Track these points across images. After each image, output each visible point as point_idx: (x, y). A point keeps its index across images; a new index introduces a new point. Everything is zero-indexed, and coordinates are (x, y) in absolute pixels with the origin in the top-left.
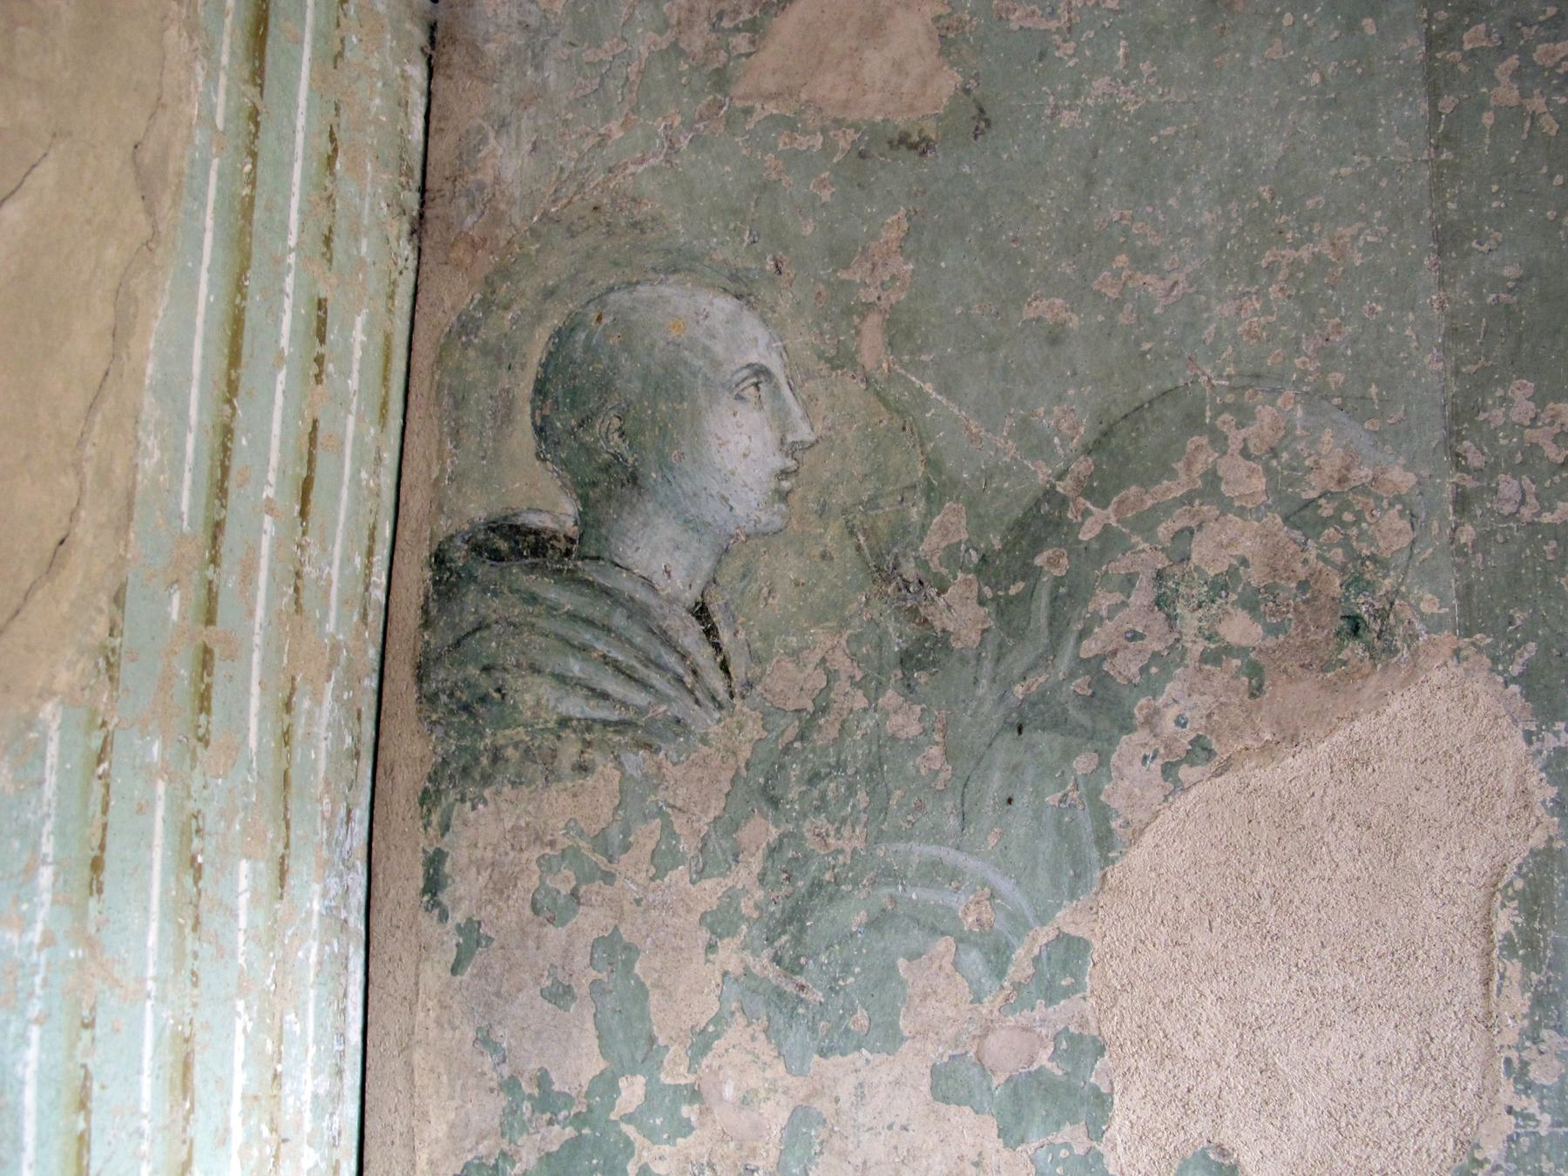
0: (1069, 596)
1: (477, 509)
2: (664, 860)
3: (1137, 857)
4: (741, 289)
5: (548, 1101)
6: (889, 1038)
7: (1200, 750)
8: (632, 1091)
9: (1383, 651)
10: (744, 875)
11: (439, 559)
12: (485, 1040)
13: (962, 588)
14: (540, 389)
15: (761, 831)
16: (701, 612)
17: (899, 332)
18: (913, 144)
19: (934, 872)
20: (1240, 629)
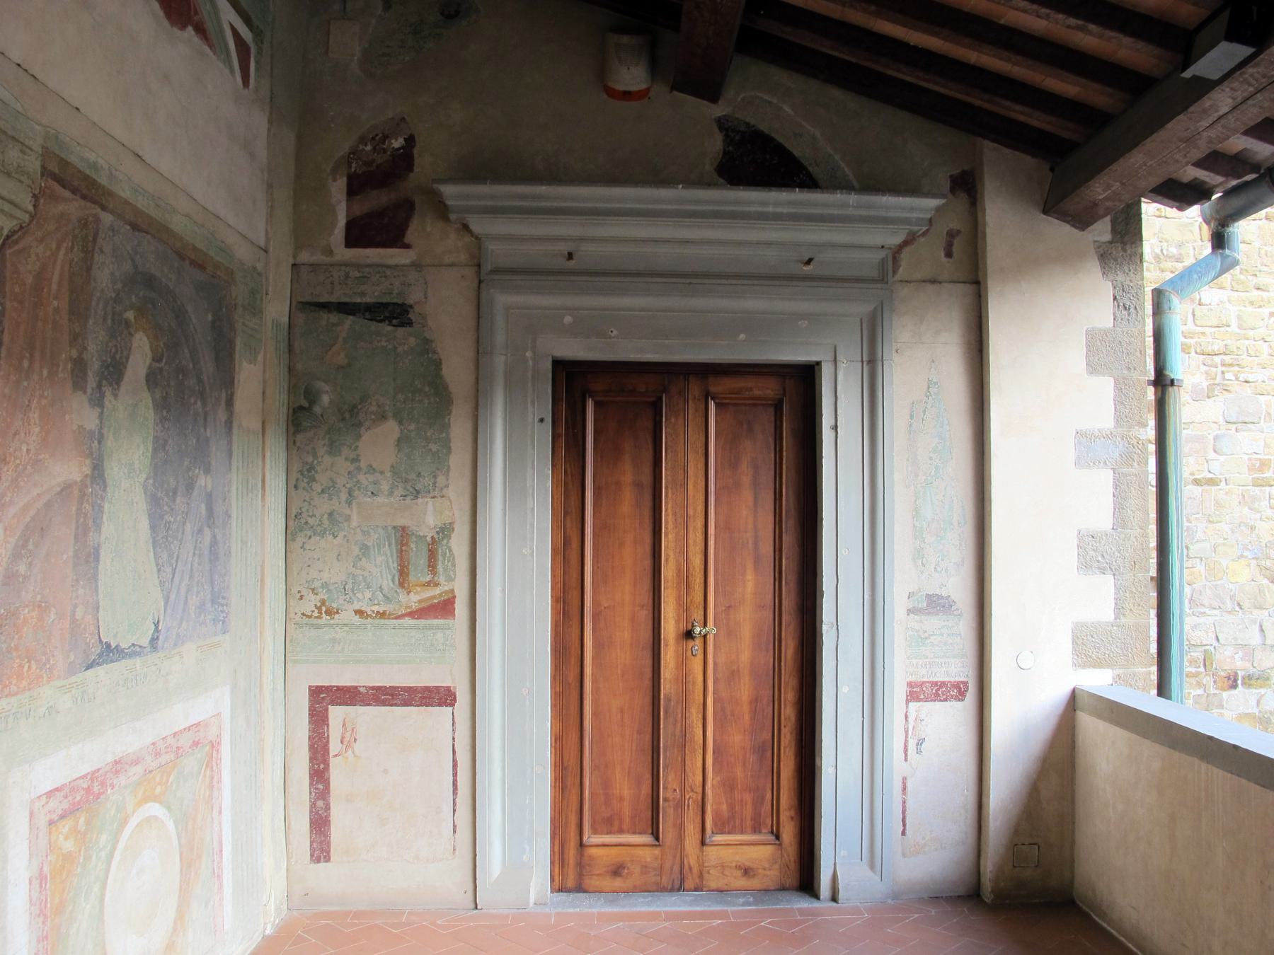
0: (358, 413)
1: (297, 404)
2: (318, 439)
3: (363, 438)
4: (326, 382)
5: (307, 463)
6: (340, 455)
7: (369, 428)
8: (316, 462)
9: (386, 419)
10: (327, 440)
11: (294, 410)
12: (300, 458)
13: (347, 413)
14: (305, 392)
15: (327, 437)
16: (322, 415)
17: (341, 388)
18: (343, 367)
19: (345, 440)
20: (373, 417)
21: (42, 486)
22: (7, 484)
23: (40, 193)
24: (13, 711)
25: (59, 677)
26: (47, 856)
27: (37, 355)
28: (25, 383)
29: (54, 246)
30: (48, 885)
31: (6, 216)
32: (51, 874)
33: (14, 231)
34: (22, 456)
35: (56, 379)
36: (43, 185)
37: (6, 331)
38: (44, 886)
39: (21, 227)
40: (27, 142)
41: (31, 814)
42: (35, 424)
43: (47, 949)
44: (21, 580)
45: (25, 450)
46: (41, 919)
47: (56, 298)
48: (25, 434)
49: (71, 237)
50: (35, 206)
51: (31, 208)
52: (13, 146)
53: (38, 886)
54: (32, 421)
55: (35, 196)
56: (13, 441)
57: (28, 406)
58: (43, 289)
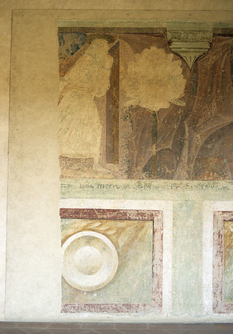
21: (219, 123)
22: (201, 124)
23: (213, 42)
24: (205, 185)
25: (229, 179)
26: (222, 229)
27: (215, 87)
28: (209, 96)
29: (221, 55)
30: (223, 238)
31: (197, 52)
32: (224, 235)
33: (201, 56)
34: (208, 116)
35: (225, 92)
36: (214, 39)
37: (199, 83)
38: (221, 237)
39: (204, 54)
40: (205, 30)
41: (214, 215)
42: (215, 106)
43: (222, 256)
44: (209, 149)
45: (210, 114)
46: (219, 246)
47: (224, 69)
48: (210, 109)
49: (230, 50)
50: (210, 46)
51: (209, 47)
52: (199, 33)
53: (218, 237)
54: (213, 106)
55: (210, 43)
56: (204, 112)
57: (211, 102)
58: (216, 68)
